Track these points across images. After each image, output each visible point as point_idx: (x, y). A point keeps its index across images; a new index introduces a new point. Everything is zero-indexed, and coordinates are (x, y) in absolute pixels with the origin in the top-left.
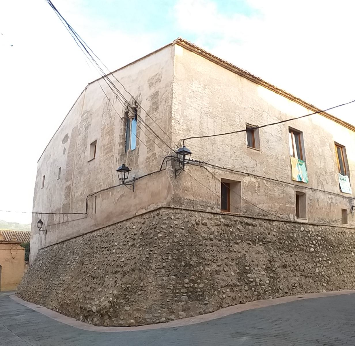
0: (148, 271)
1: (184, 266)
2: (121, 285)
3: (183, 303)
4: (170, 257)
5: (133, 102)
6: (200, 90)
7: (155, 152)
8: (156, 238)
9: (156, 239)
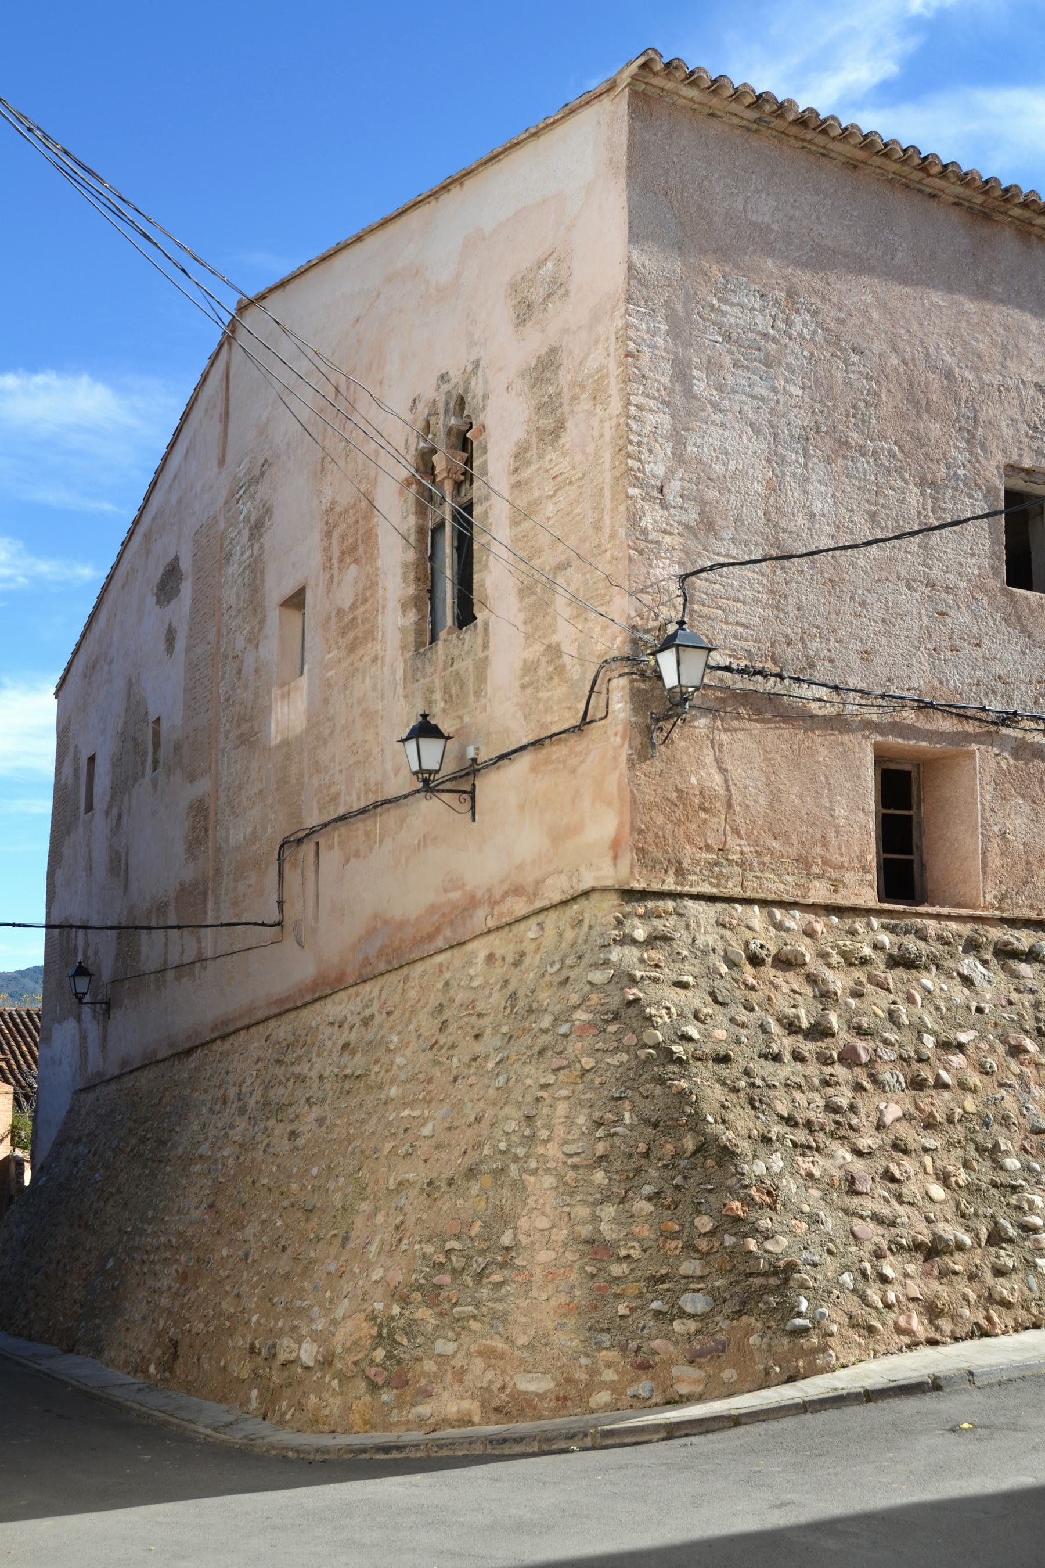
0: (532, 1179)
1: (694, 1154)
2: (420, 1242)
3: (692, 1326)
4: (627, 1115)
5: (447, 404)
6: (762, 322)
7: (555, 639)
8: (564, 1029)
9: (565, 1036)
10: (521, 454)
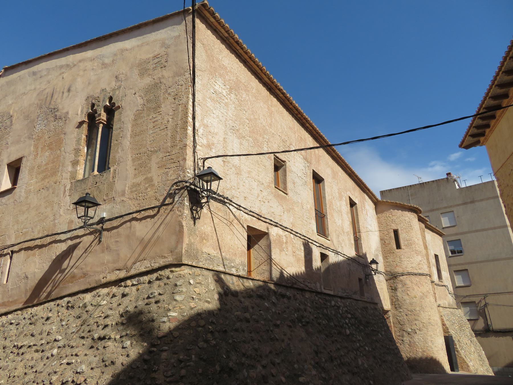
1: (220, 371)
4: (193, 356)
10: (138, 116)
